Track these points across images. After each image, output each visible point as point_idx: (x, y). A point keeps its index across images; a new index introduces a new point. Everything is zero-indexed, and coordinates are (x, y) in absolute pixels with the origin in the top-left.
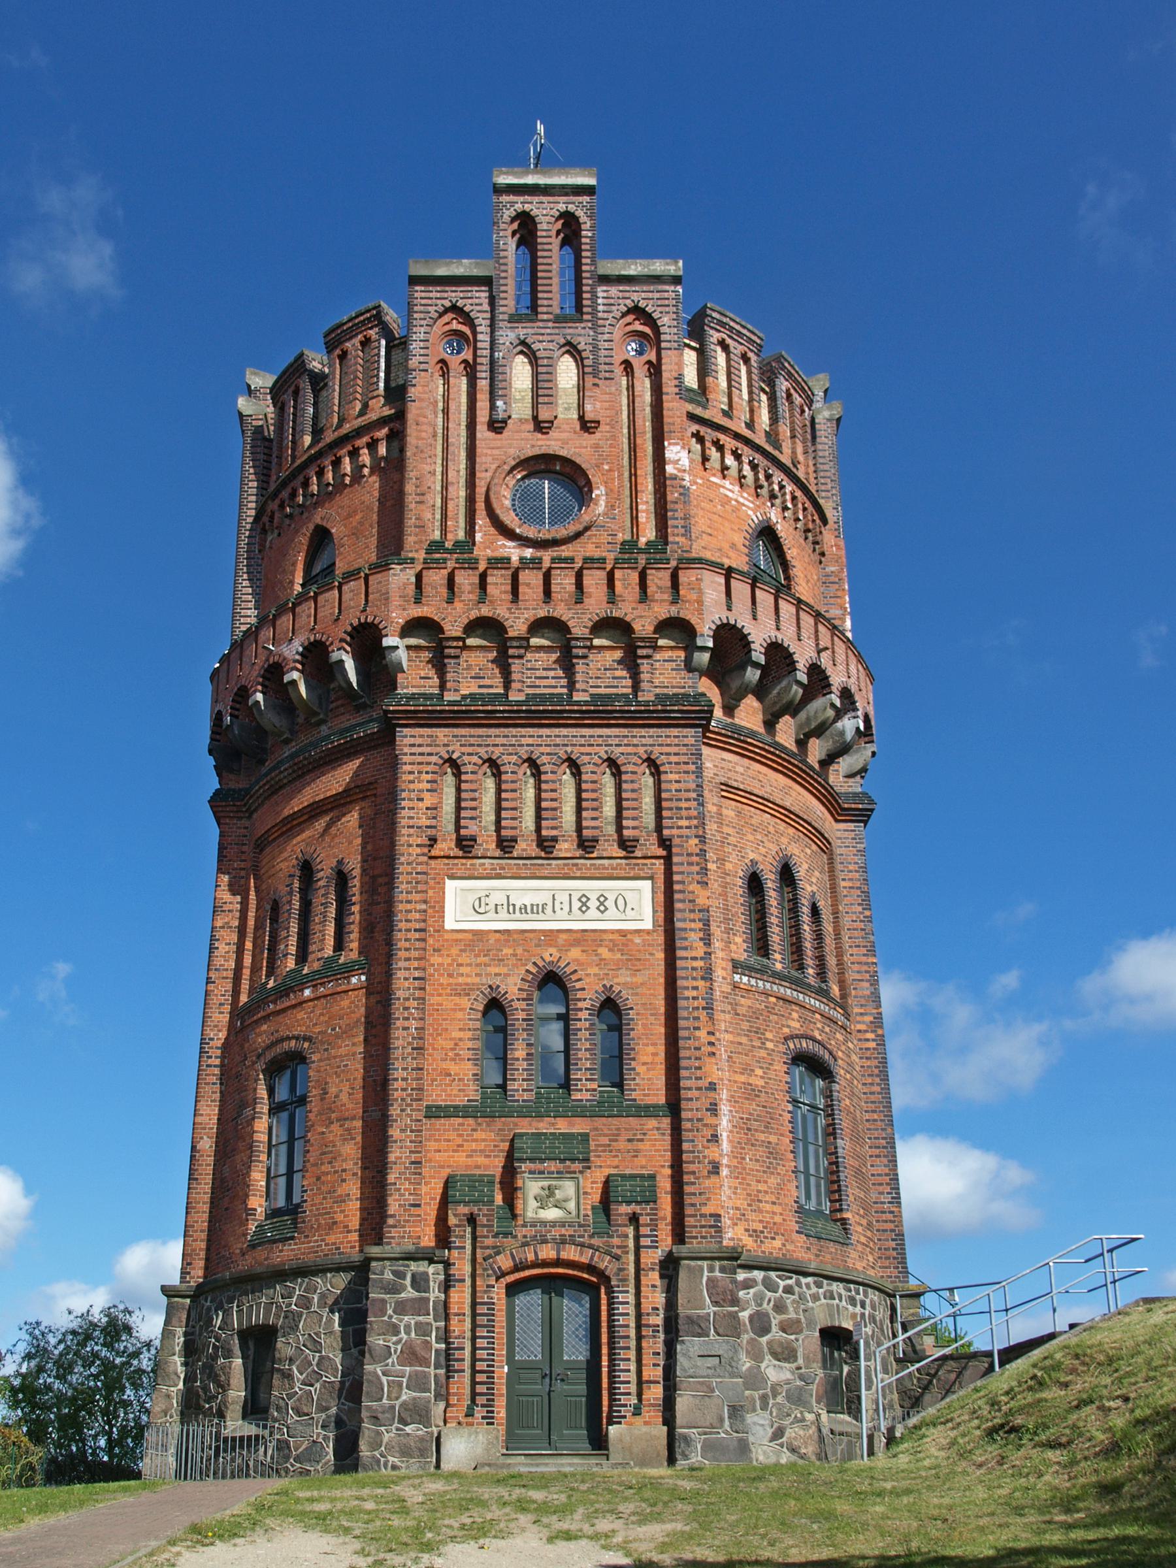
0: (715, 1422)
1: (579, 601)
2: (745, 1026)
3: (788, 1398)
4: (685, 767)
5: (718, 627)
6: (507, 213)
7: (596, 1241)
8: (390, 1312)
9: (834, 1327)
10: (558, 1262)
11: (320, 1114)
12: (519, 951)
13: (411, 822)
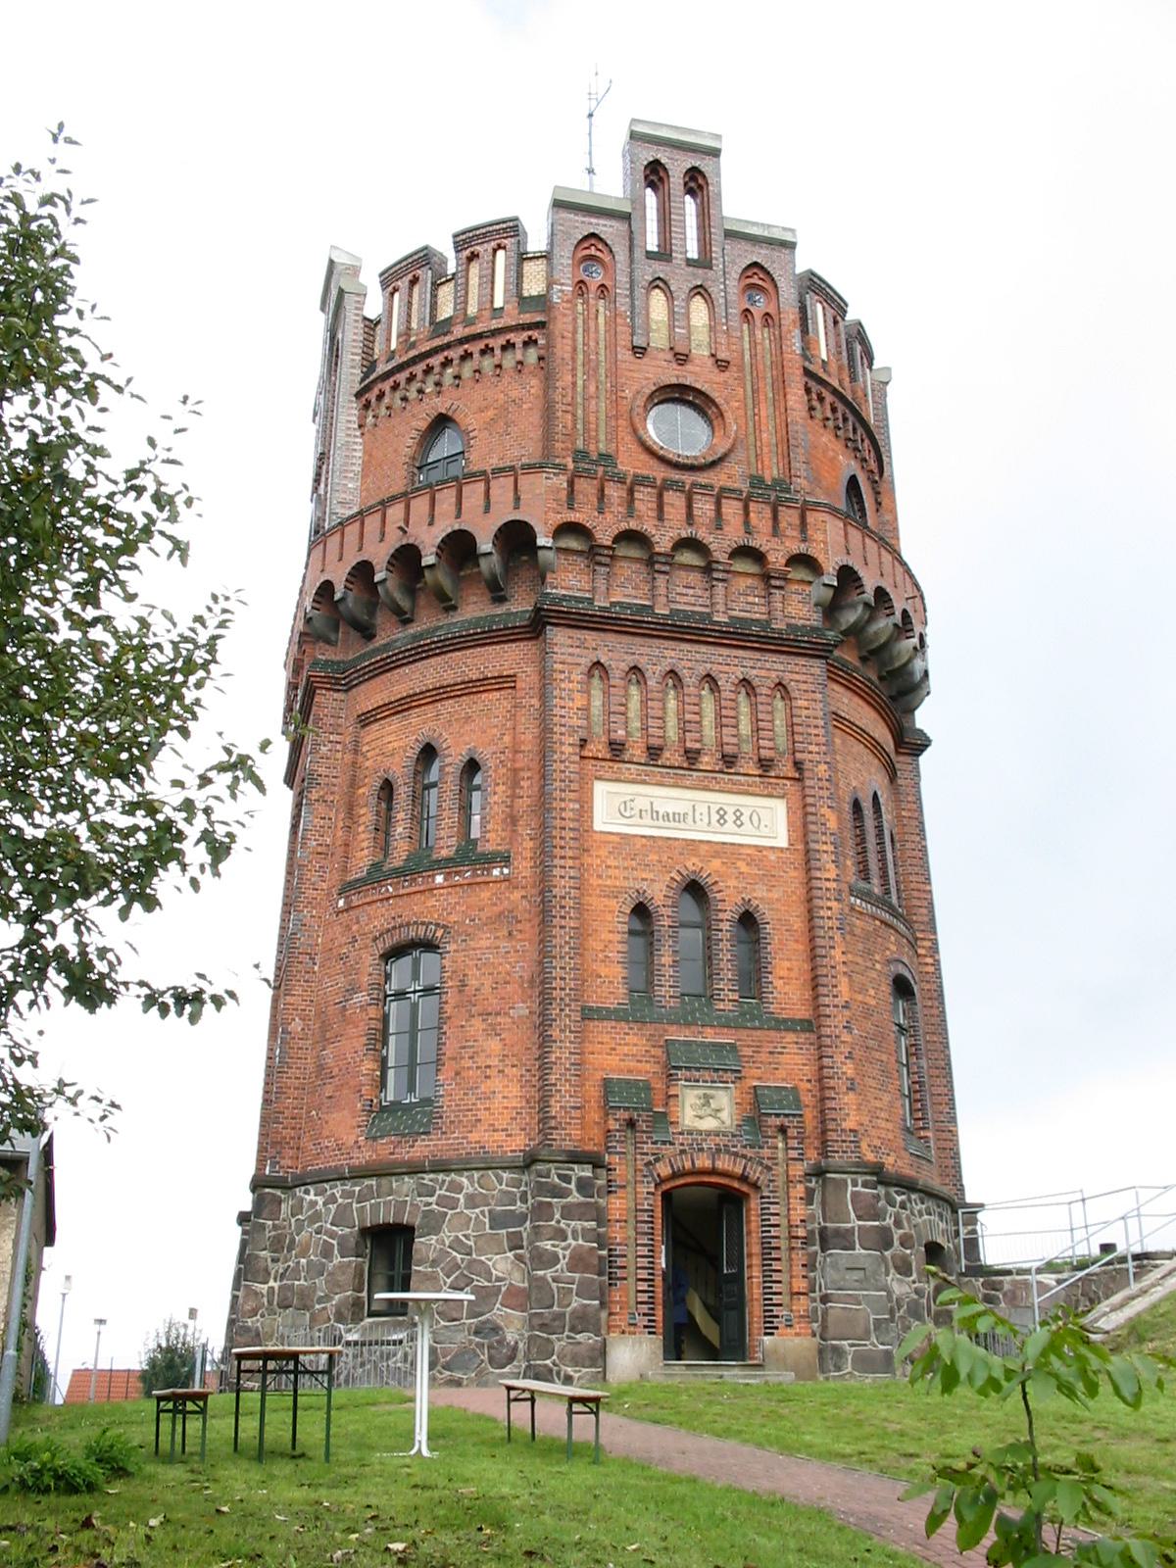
1: (719, 528)
7: (749, 1152)
8: (557, 1216)
10: (713, 1172)
13: (563, 721)
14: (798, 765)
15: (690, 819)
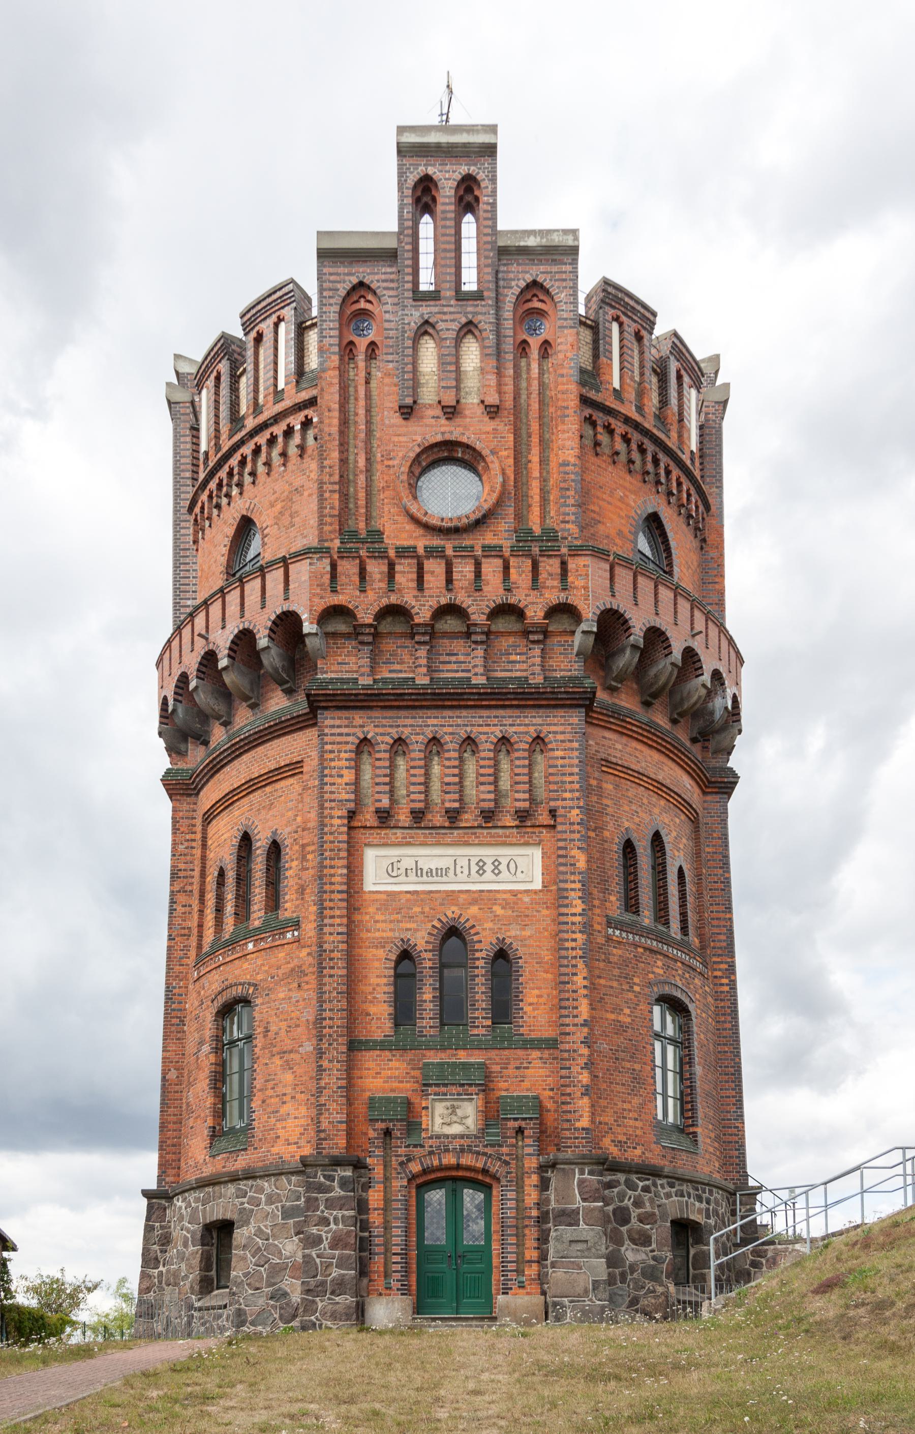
0: (581, 1292)
2: (616, 972)
3: (644, 1274)
4: (568, 745)
5: (602, 612)
6: (411, 177)
9: (682, 1219)
11: (263, 1048)
12: (427, 909)
13: (333, 797)
14: (553, 813)
15: (452, 871)
